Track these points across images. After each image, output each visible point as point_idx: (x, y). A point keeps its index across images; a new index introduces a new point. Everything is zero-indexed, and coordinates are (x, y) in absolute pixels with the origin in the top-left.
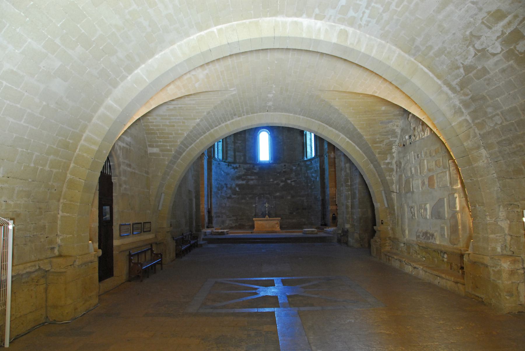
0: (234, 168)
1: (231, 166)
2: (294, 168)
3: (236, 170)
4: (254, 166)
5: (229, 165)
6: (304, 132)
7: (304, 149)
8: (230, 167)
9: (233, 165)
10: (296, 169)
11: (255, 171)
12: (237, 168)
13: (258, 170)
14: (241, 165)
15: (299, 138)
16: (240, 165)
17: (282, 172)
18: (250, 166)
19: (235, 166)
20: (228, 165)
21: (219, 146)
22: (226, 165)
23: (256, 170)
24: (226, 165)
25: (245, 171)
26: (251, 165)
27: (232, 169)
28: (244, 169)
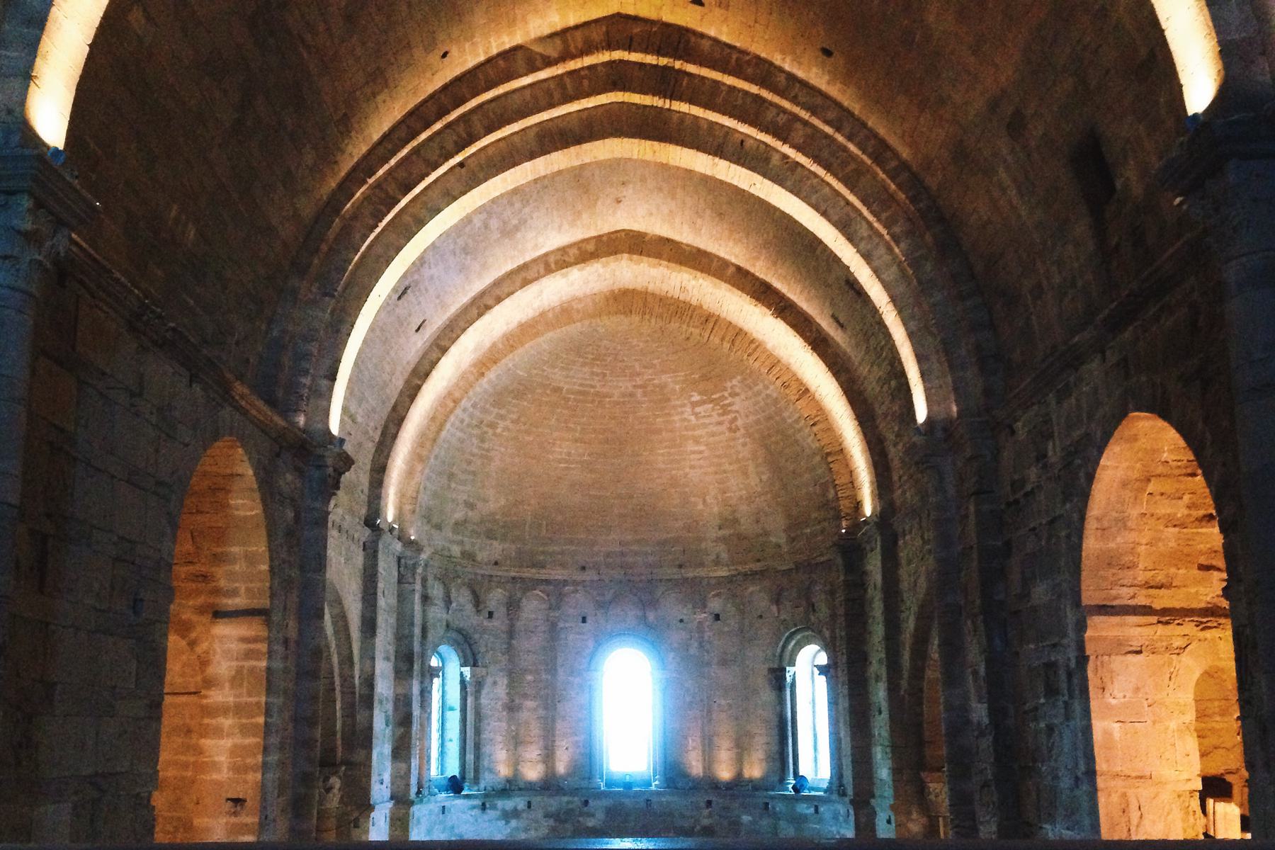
0: (507, 816)
1: (494, 807)
2: (746, 818)
3: (514, 823)
4: (586, 803)
5: (484, 804)
6: (787, 675)
7: (787, 744)
8: (491, 814)
9: (500, 803)
10: (754, 822)
11: (591, 823)
12: (515, 814)
13: (600, 815)
14: (536, 800)
15: (767, 695)
16: (529, 803)
17: (698, 828)
18: (568, 803)
19: (508, 804)
20: (483, 807)
21: (448, 725)
22: (474, 807)
23: (593, 815)
24: (474, 807)
25: (551, 822)
26: (576, 799)
27: (497, 819)
28: (547, 816)
